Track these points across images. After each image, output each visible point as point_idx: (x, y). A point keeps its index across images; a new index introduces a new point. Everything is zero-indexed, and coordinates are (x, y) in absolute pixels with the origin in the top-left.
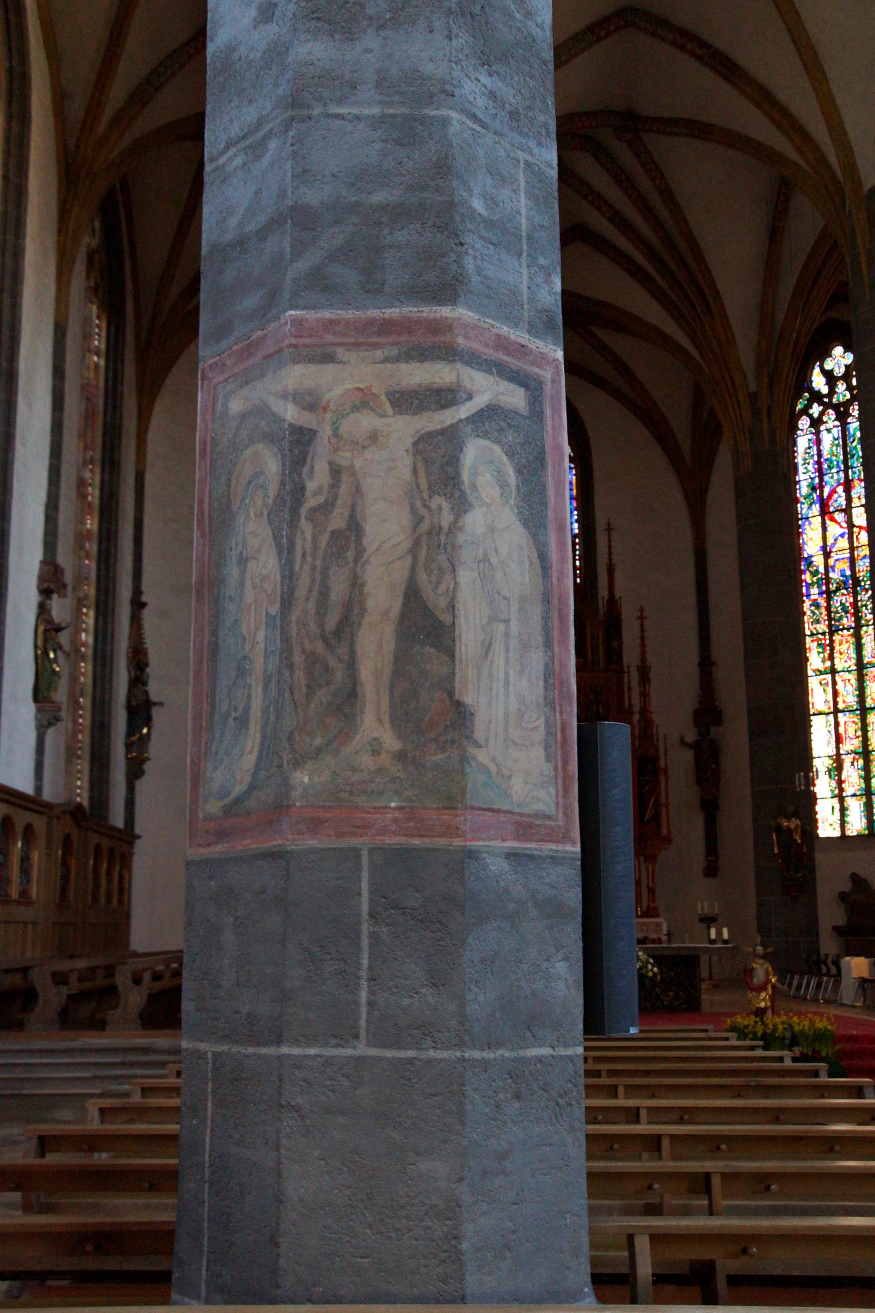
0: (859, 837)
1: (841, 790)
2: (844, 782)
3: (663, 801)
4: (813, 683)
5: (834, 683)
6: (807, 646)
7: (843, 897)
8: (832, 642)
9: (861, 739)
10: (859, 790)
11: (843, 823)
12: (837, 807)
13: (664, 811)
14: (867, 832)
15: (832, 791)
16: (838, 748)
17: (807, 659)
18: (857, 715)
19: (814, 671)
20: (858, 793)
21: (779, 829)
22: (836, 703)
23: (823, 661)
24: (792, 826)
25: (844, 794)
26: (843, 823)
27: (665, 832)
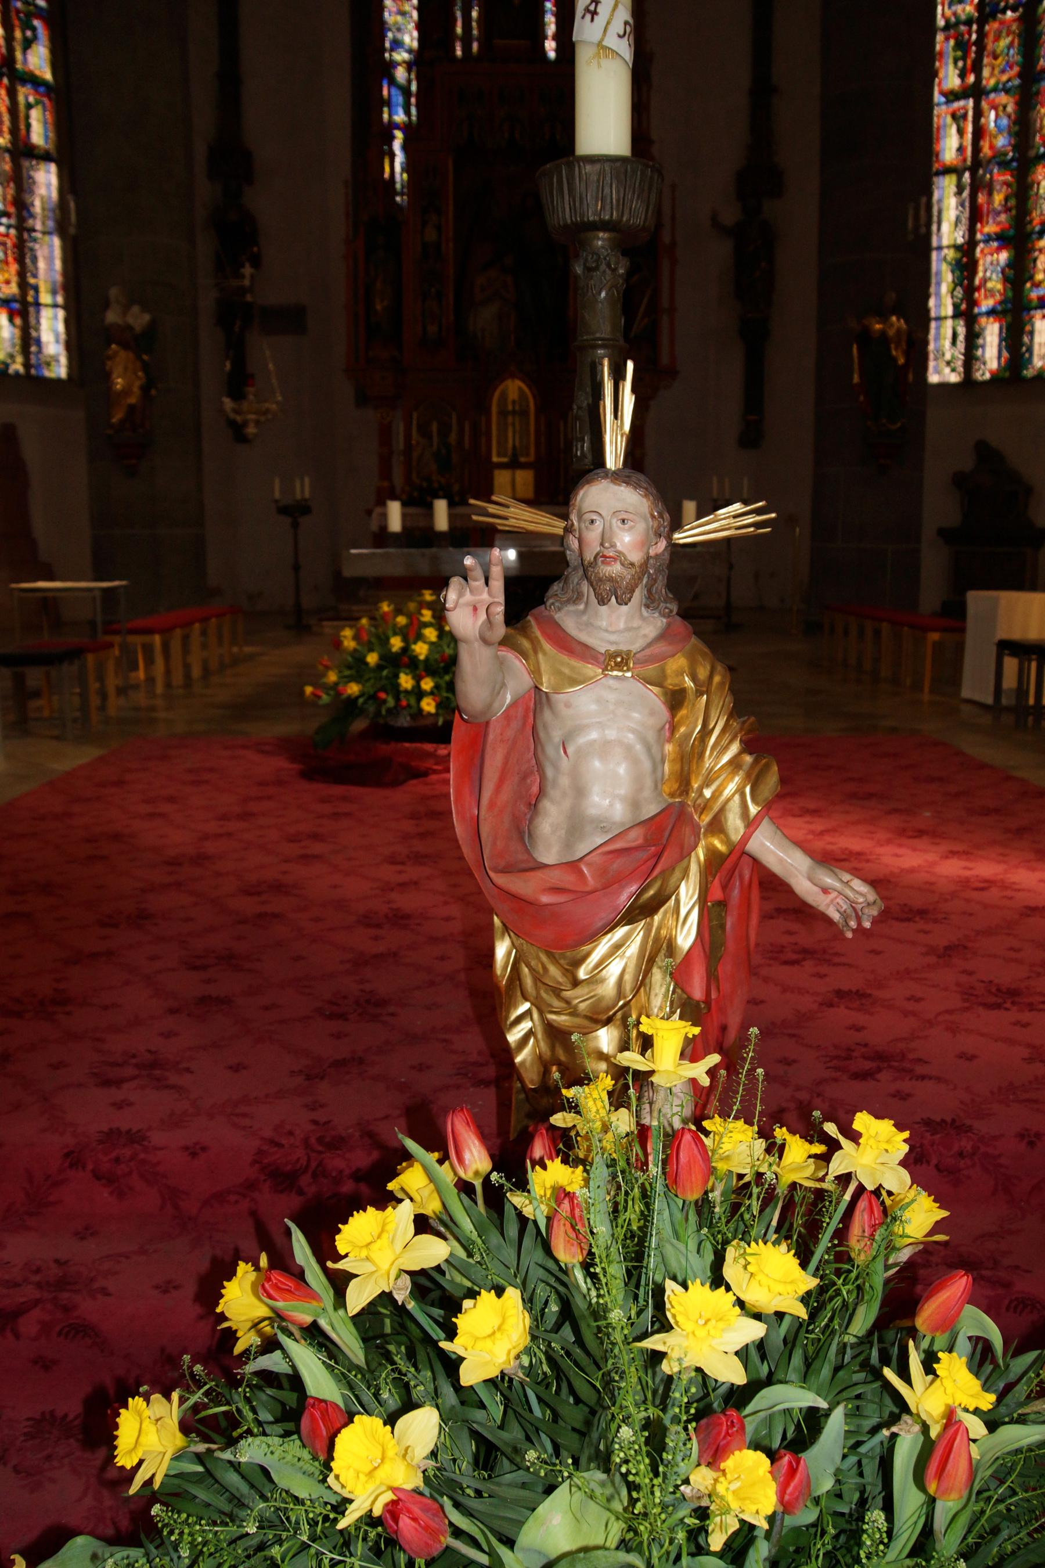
0: (996, 379)
1: (973, 303)
2: (978, 289)
3: (665, 303)
4: (942, 113)
5: (978, 113)
6: (938, 47)
7: (959, 480)
8: (982, 34)
9: (1014, 212)
10: (1001, 303)
11: (970, 358)
12: (962, 331)
13: (665, 320)
14: (1007, 374)
15: (956, 306)
16: (972, 230)
17: (935, 74)
18: (1012, 171)
19: (943, 94)
20: (999, 308)
21: (865, 338)
22: (976, 149)
23: (962, 75)
24: (891, 332)
25: (976, 310)
26: (970, 358)
27: (665, 360)
